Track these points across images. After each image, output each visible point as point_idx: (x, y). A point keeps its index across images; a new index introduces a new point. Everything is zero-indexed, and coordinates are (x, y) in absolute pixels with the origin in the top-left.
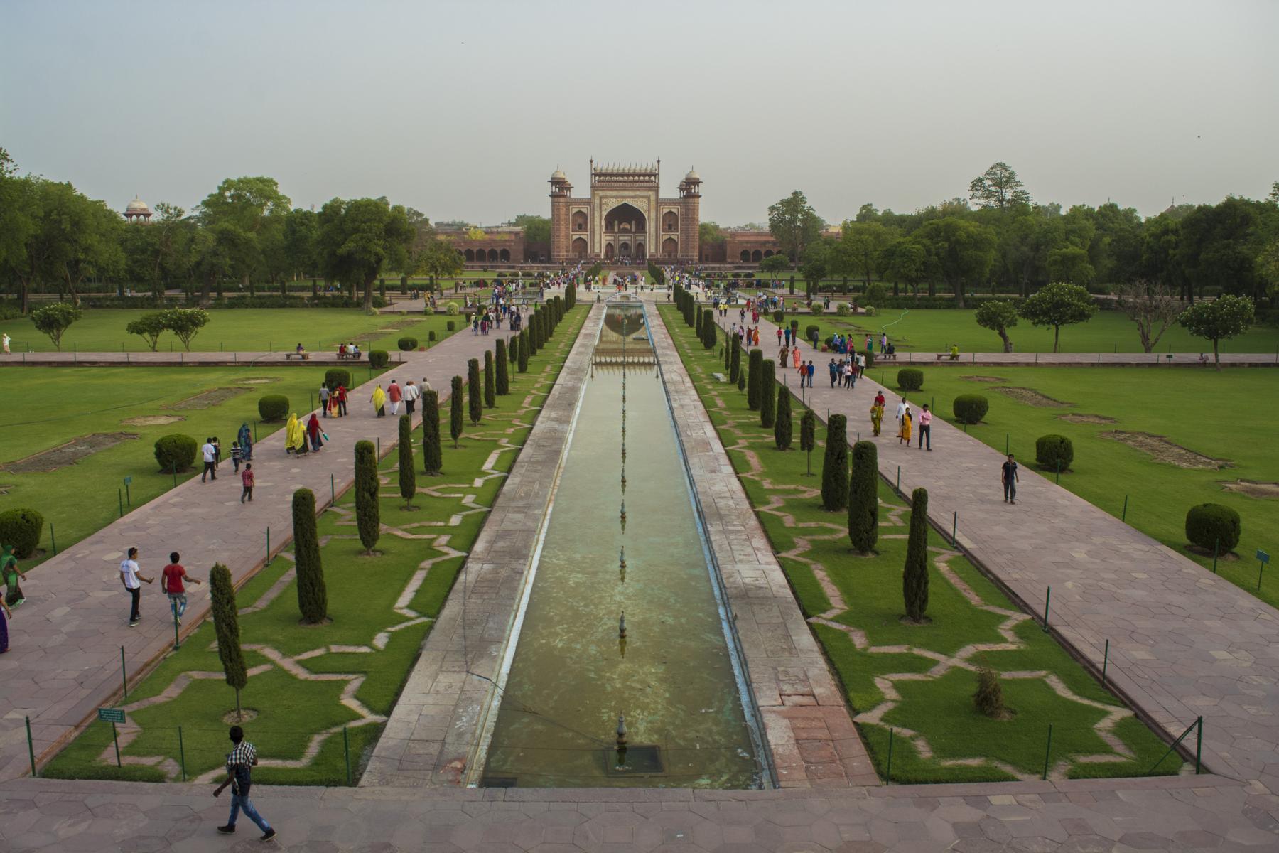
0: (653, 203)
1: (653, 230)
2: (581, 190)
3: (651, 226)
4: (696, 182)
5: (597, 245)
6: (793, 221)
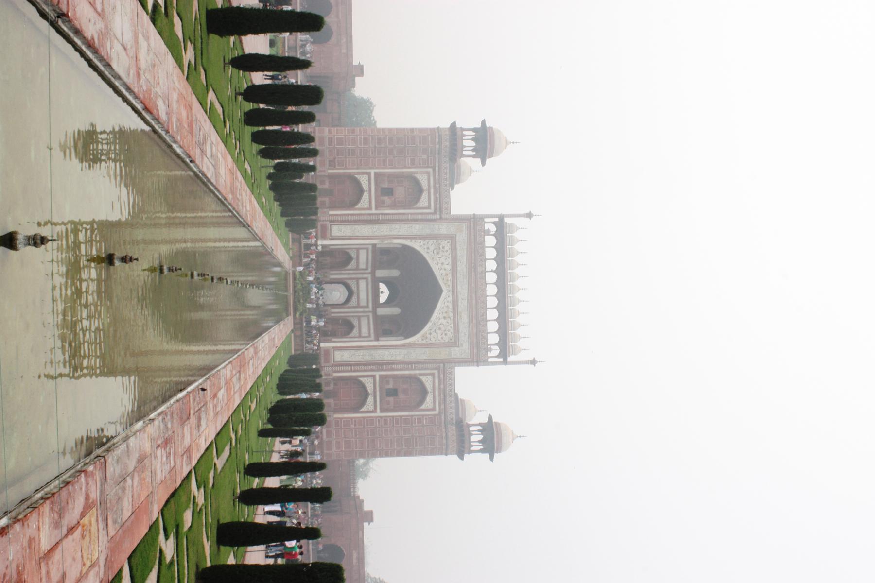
0: (442, 354)
3: (394, 350)
5: (347, 230)
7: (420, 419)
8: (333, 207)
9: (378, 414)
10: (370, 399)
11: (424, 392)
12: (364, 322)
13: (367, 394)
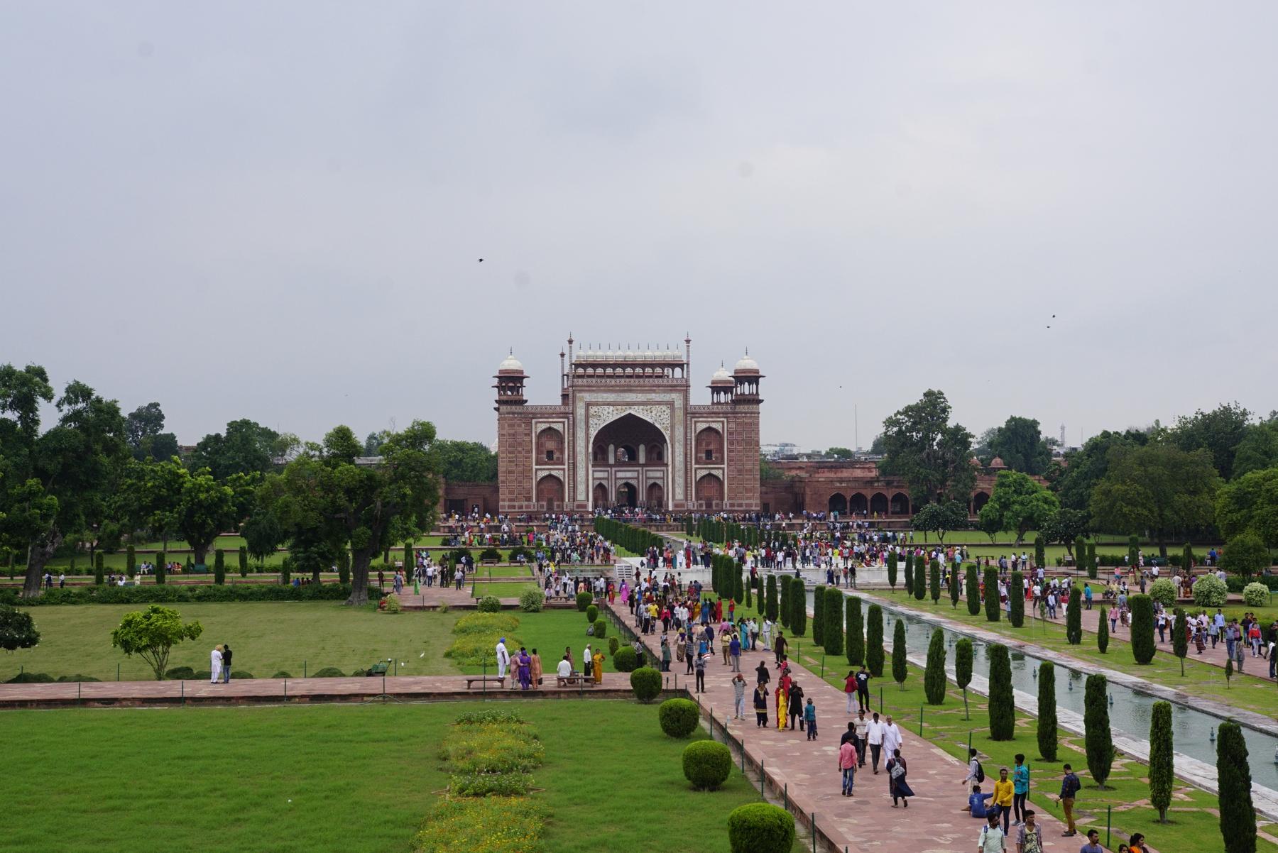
0: (679, 414)
1: (679, 459)
2: (542, 391)
3: (675, 453)
4: (752, 378)
5: (581, 488)
6: (927, 439)
7: (730, 433)
8: (563, 500)
9: (725, 466)
10: (713, 472)
11: (709, 429)
12: (651, 474)
13: (710, 474)
